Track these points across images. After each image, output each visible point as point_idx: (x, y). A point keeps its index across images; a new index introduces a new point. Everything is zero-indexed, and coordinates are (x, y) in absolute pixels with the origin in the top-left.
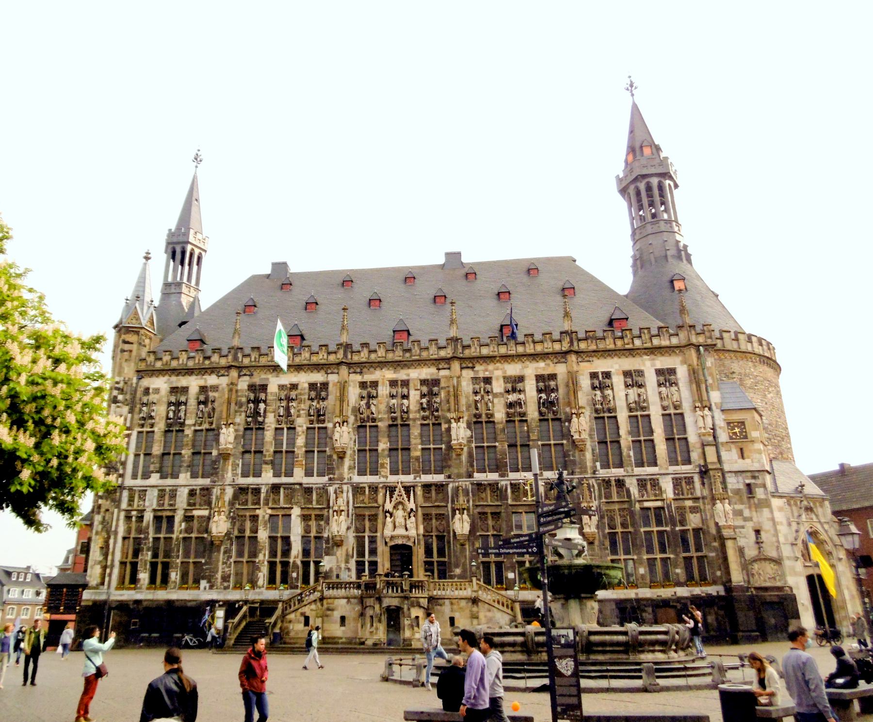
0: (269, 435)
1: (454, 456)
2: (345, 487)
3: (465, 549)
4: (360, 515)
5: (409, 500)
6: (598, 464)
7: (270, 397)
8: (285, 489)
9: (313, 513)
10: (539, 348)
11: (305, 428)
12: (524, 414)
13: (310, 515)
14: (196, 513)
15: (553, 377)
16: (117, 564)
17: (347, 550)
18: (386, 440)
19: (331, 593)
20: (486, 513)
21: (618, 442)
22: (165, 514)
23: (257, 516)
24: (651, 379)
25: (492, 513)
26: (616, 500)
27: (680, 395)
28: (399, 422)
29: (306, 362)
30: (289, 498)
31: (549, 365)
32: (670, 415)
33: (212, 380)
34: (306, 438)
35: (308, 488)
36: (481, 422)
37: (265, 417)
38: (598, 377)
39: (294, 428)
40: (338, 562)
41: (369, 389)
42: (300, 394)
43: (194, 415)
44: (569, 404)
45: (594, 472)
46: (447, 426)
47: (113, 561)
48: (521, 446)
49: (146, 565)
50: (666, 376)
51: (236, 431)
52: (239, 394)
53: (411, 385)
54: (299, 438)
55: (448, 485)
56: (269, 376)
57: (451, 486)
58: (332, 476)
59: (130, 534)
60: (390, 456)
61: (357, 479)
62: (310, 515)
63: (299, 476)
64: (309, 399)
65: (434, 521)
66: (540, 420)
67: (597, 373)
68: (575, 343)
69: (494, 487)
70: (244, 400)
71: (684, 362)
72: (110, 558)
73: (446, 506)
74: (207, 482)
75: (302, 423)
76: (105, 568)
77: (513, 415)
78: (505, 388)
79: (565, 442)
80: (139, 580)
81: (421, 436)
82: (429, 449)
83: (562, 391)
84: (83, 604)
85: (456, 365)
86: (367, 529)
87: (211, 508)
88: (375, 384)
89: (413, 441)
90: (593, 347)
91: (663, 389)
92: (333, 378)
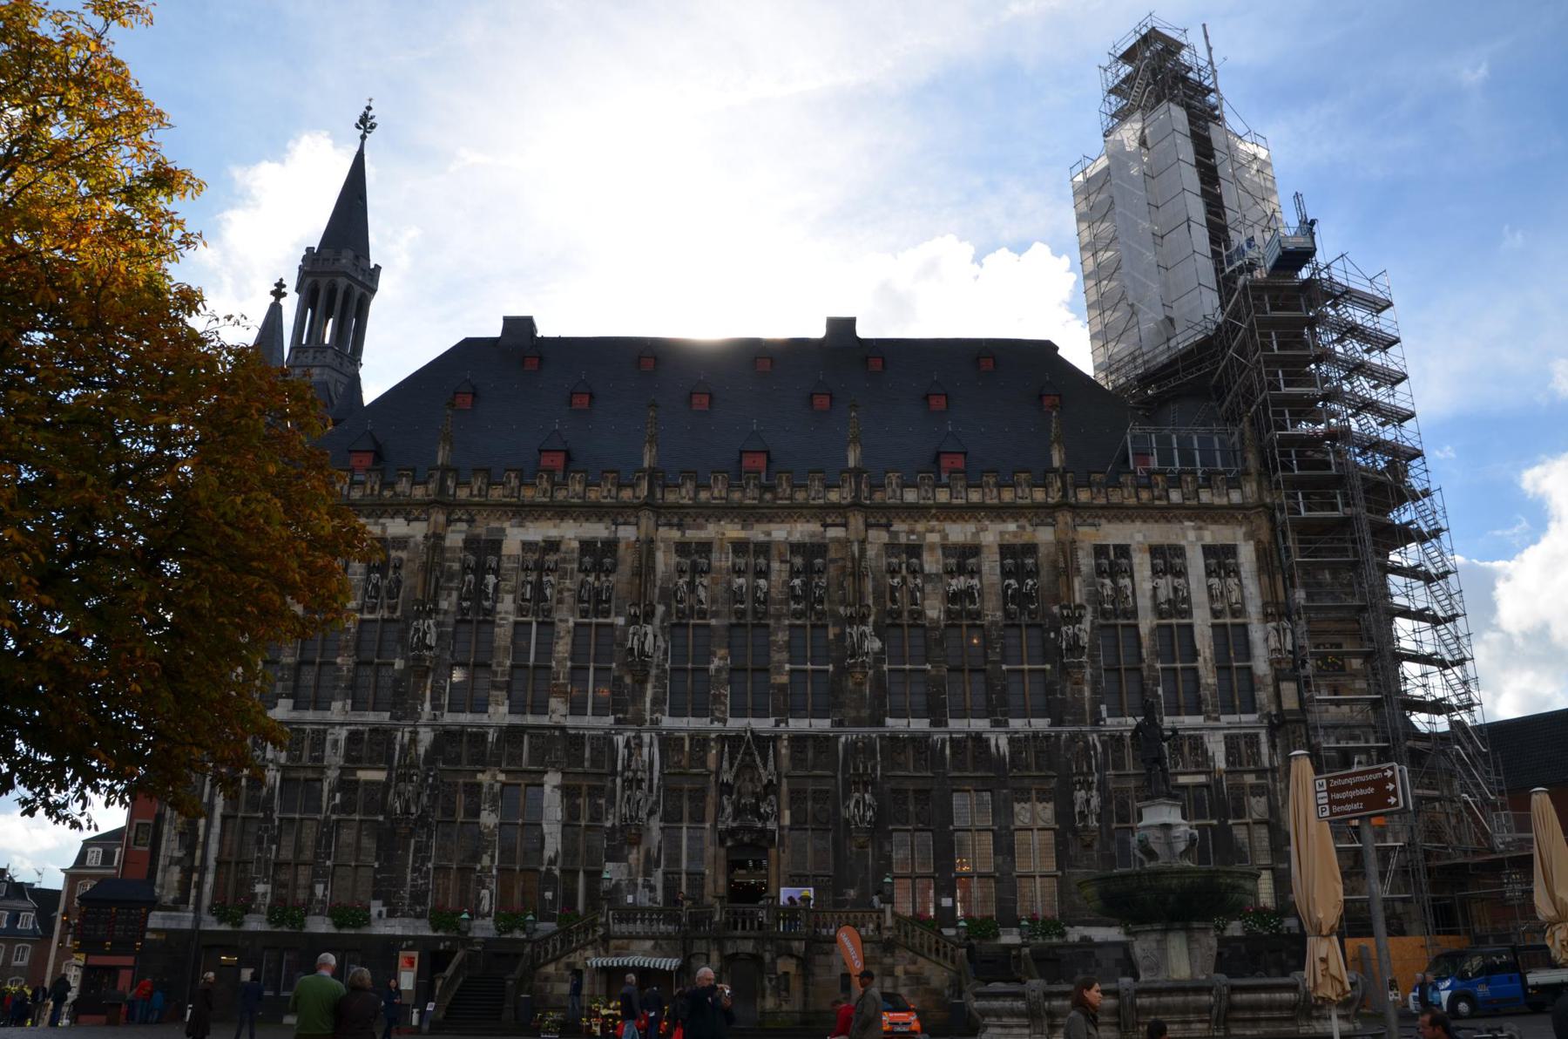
0: (503, 634)
1: (850, 684)
2: (646, 737)
6: (1103, 708)
7: (506, 564)
8: (531, 736)
9: (585, 784)
11: (571, 624)
12: (978, 614)
13: (580, 787)
14: (364, 775)
15: (1031, 549)
16: (212, 863)
17: (648, 851)
18: (722, 652)
19: (624, 928)
20: (906, 791)
21: (1139, 670)
22: (302, 775)
23: (480, 785)
24: (1196, 563)
25: (915, 791)
26: (1132, 771)
27: (1242, 591)
28: (749, 619)
29: (575, 500)
32: (1224, 625)
34: (574, 644)
35: (576, 736)
36: (901, 626)
37: (495, 602)
38: (1107, 557)
39: (552, 624)
40: (630, 873)
41: (696, 557)
42: (564, 560)
43: (360, 593)
44: (1056, 600)
46: (837, 630)
47: (204, 858)
48: (962, 671)
49: (267, 869)
50: (1220, 559)
51: (438, 624)
52: (448, 555)
53: (774, 552)
54: (561, 642)
55: (837, 738)
56: (506, 525)
57: (843, 739)
59: (236, 809)
60: (730, 682)
61: (667, 722)
63: (558, 713)
64: (580, 570)
65: (810, 804)
67: (1107, 546)
68: (1071, 493)
69: (919, 743)
70: (456, 566)
71: (1249, 536)
72: (198, 853)
73: (835, 777)
74: (385, 716)
75: (566, 620)
76: (187, 872)
77: (959, 614)
78: (945, 565)
79: (1048, 667)
80: (255, 895)
81: (789, 645)
82: (805, 671)
83: (1043, 573)
84: (148, 936)
87: (390, 769)
88: (705, 547)
89: (776, 657)
90: (1103, 501)
91: (1215, 581)
92: (627, 533)
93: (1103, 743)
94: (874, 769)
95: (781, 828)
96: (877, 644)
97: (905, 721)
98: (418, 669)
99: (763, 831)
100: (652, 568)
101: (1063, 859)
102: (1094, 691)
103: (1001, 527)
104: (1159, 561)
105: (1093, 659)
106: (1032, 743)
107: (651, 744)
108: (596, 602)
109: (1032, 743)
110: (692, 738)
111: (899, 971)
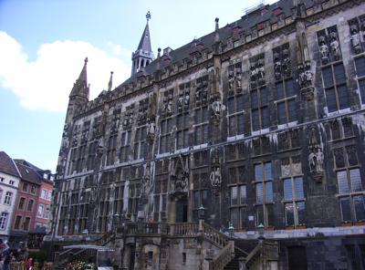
0: (119, 137)
2: (152, 163)
10: (275, 28)
12: (264, 82)
15: (286, 46)
18: (174, 126)
20: (235, 168)
21: (345, 84)
25: (239, 167)
30: (125, 174)
31: (282, 38)
33: (100, 113)
45: (322, 117)
61: (158, 156)
63: (131, 162)
66: (276, 84)
69: (240, 144)
75: (135, 128)
77: (255, 85)
85: (217, 61)
88: (172, 91)
90: (320, 10)
93: (327, 128)
94: (222, 160)
96: (224, 108)
98: (100, 155)
99: (183, 193)
100: (156, 104)
101: (307, 191)
102: (320, 101)
103: (272, 42)
104: (355, 27)
105: (318, 85)
106: (289, 135)
108: (142, 121)
109: (289, 135)
111: (204, 252)
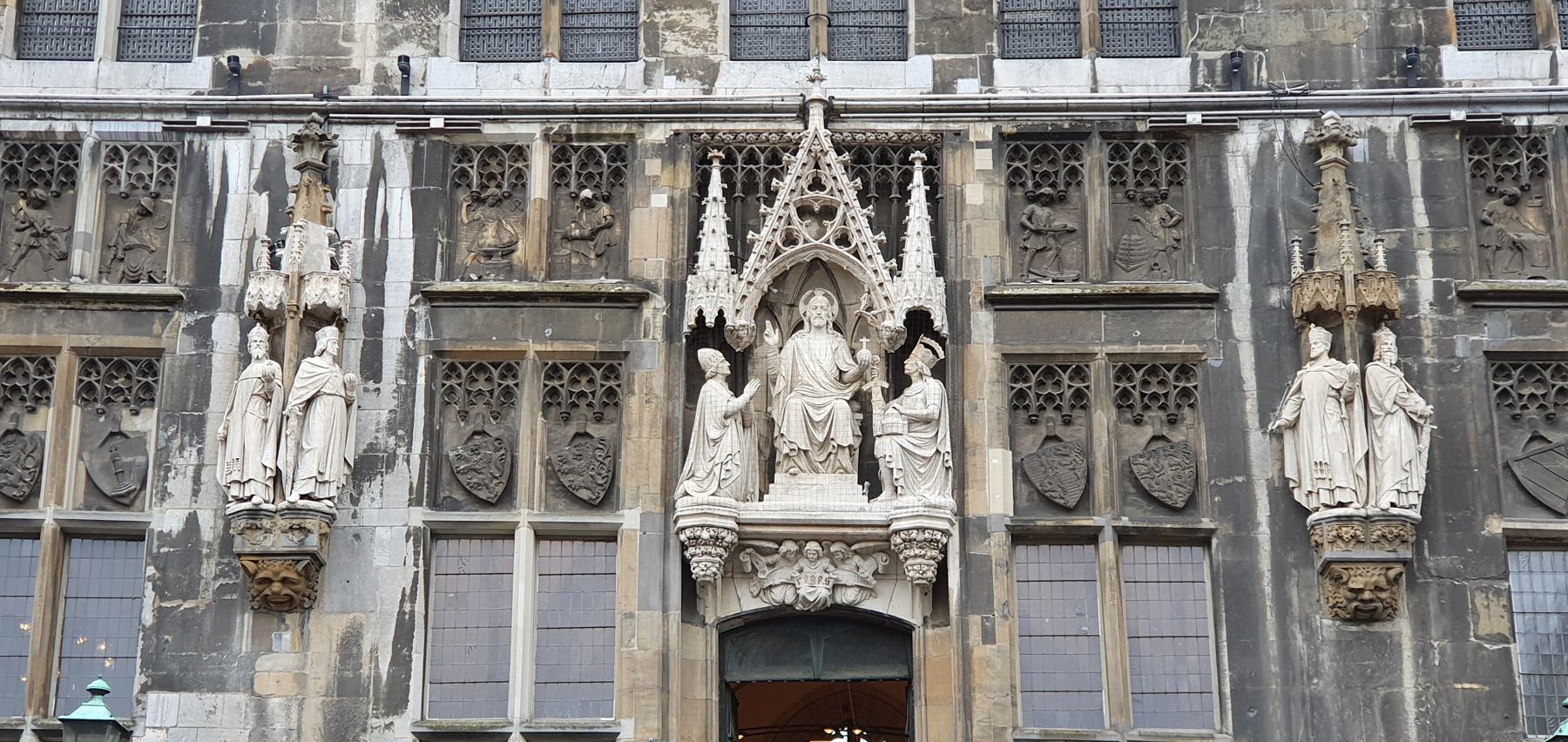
2: (354, 145)
3: (1387, 648)
4: (480, 367)
5: (894, 250)
13: (43, 360)
35: (40, 146)
58: (247, 57)
61: (448, 79)
62: (43, 360)
65: (1103, 417)
73: (1212, 301)
86: (530, 474)
95: (970, 527)
97: (1536, 62)
107: (379, 173)
110: (560, 155)
